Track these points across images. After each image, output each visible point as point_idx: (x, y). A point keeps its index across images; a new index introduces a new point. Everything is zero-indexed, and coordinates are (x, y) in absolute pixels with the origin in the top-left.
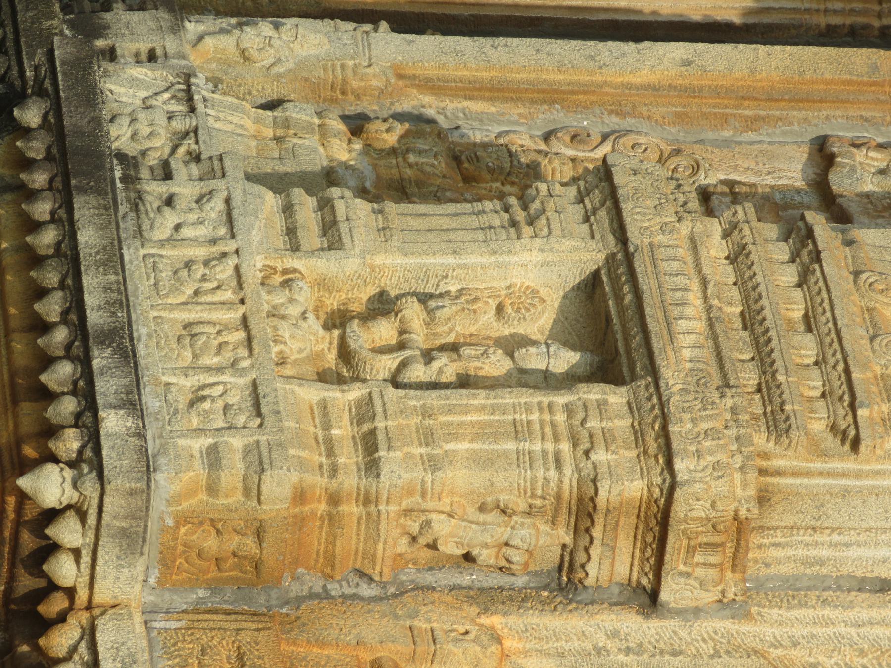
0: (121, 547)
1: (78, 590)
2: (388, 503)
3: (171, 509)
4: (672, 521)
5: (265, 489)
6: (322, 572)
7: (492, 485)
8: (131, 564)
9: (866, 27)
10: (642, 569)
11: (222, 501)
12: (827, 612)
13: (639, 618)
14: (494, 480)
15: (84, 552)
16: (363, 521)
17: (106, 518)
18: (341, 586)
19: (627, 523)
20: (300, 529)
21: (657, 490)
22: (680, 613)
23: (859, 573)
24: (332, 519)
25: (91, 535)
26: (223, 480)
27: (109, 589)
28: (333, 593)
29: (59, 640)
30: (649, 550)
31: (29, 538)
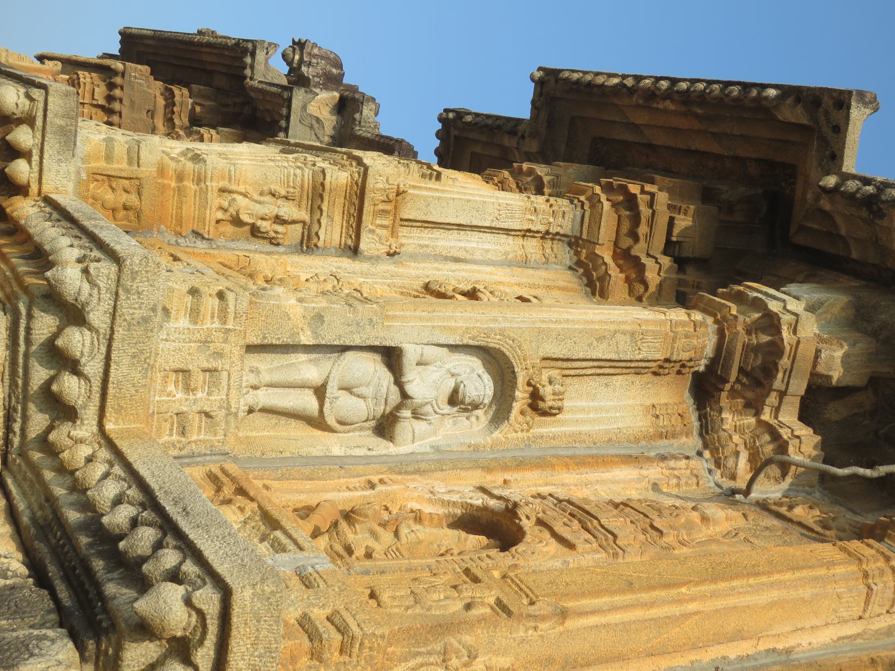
0: (60, 143)
3: (84, 166)
4: (367, 191)
5: (143, 155)
6: (175, 231)
10: (347, 233)
11: (116, 166)
12: (436, 265)
13: (350, 261)
14: (267, 174)
15: (34, 151)
16: (198, 194)
17: (50, 115)
19: (340, 201)
20: (162, 194)
21: (357, 175)
23: (444, 253)
24: (180, 190)
25: (39, 135)
26: (116, 148)
27: (52, 181)
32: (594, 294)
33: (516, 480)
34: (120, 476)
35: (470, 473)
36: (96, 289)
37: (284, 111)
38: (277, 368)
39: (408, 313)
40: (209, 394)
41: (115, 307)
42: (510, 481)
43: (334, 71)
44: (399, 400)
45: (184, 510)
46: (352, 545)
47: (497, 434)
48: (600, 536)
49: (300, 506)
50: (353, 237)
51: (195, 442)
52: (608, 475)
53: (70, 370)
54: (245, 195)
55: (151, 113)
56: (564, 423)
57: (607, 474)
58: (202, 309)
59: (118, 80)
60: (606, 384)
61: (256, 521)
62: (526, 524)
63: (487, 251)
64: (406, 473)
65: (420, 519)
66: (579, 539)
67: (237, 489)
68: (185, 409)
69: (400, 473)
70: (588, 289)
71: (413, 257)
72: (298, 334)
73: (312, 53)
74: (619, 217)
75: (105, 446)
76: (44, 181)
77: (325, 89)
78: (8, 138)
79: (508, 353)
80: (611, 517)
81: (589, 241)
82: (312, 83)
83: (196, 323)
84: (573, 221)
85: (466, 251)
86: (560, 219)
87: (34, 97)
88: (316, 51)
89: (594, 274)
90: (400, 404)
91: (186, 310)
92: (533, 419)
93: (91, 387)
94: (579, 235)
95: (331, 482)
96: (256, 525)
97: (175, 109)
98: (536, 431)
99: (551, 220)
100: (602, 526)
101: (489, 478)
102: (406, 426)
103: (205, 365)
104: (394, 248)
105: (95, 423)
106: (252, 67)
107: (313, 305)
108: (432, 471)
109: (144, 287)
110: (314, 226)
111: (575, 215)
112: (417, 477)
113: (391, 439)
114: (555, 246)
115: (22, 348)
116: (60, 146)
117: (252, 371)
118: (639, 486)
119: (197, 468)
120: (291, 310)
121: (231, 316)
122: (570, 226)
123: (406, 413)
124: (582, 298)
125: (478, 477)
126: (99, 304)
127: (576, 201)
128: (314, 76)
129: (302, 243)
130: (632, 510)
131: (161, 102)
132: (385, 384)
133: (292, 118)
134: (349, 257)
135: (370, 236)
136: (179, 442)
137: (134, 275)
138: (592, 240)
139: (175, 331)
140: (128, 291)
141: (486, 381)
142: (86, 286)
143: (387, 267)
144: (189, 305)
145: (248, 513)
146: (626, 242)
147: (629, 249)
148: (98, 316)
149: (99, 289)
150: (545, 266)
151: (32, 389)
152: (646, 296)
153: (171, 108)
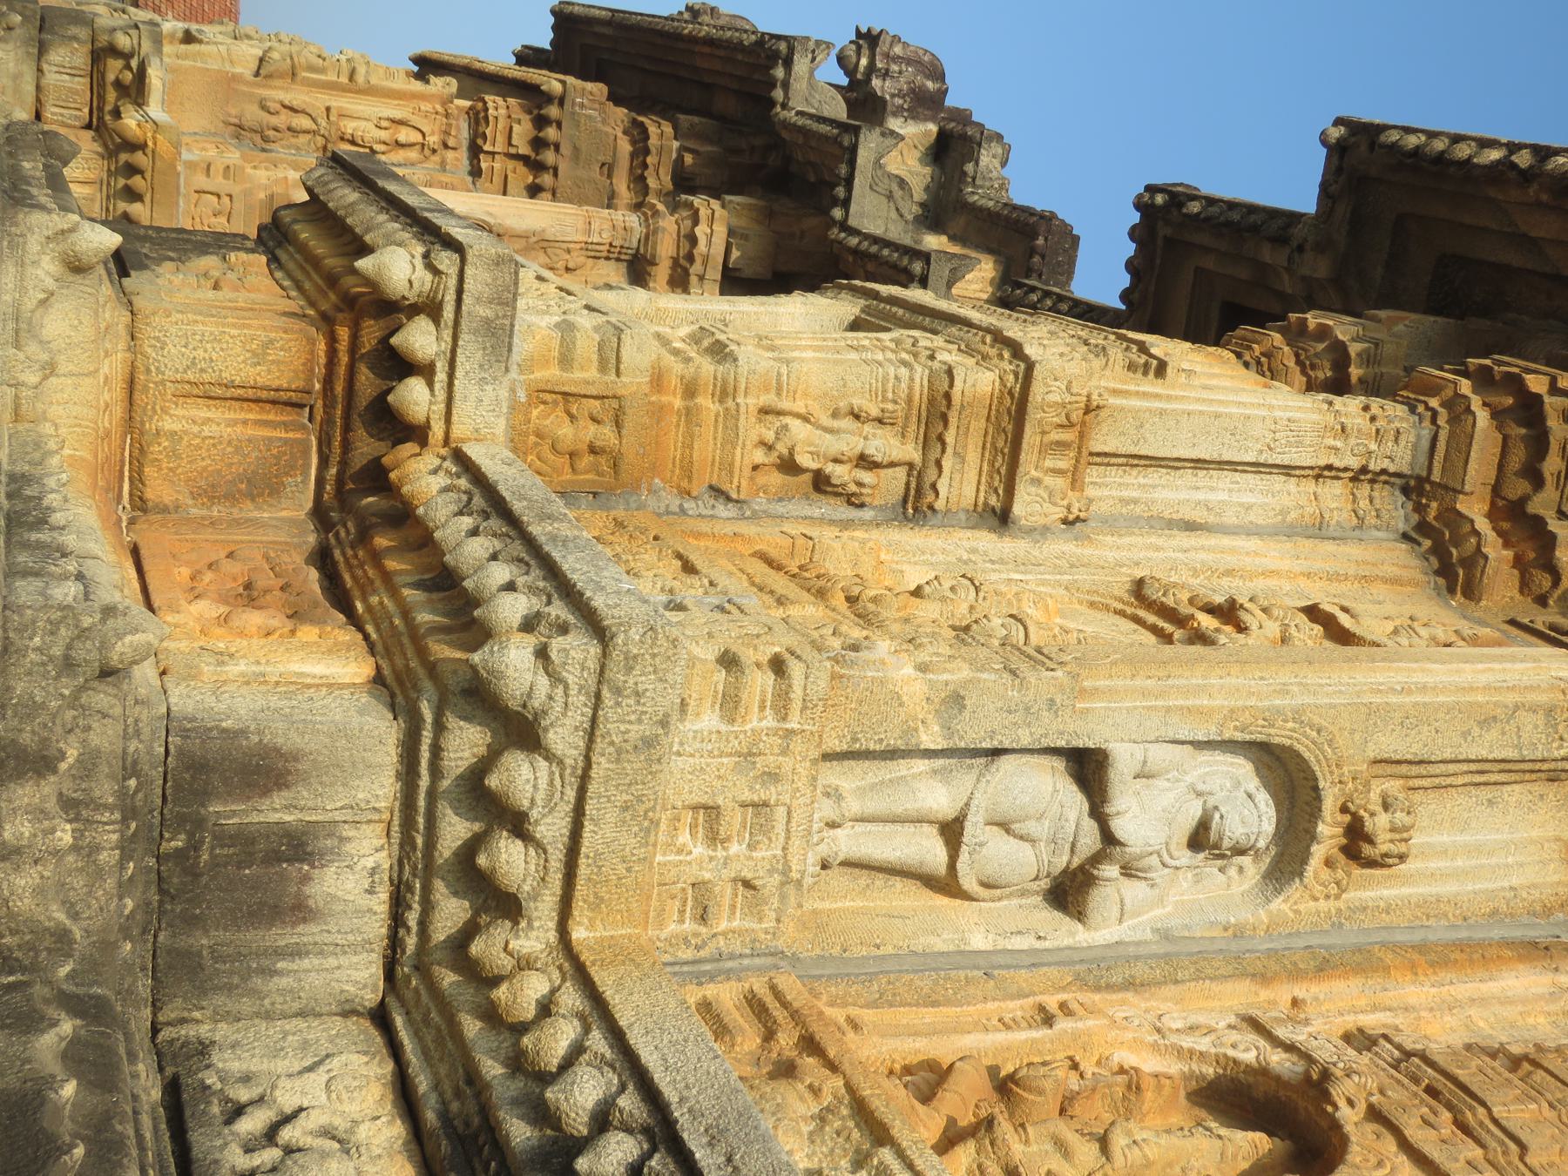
0: (484, 349)
1: (432, 423)
2: (745, 396)
3: (522, 378)
6: (679, 487)
7: (844, 386)
8: (495, 379)
10: (990, 485)
11: (578, 375)
12: (1153, 539)
13: (993, 536)
16: (721, 419)
17: (467, 299)
18: (698, 506)
20: (658, 423)
21: (1011, 377)
22: (1031, 531)
23: (1166, 515)
24: (690, 415)
25: (447, 335)
26: (579, 343)
27: (469, 417)
28: (690, 513)
29: (415, 466)
30: (1000, 459)
31: (367, 378)
32: (1451, 590)
33: (1316, 999)
34: (603, 1056)
35: (1229, 986)
36: (561, 687)
37: (843, 170)
38: (873, 787)
39: (1120, 682)
40: (752, 847)
41: (594, 720)
42: (1303, 1001)
43: (930, 85)
44: (1099, 846)
45: (729, 1160)
46: (1021, 1169)
47: (1278, 904)
48: (1493, 1144)
49: (913, 1060)
50: (1001, 492)
51: (724, 934)
52: (1492, 987)
53: (510, 827)
54: (805, 419)
55: (609, 169)
56: (1408, 879)
57: (1491, 984)
58: (744, 696)
59: (553, 111)
60: (1489, 801)
61: (843, 1119)
62: (1349, 1117)
63: (1249, 508)
64: (1110, 988)
65: (1138, 1088)
66: (1457, 1160)
67: (802, 1038)
68: (707, 876)
69: (1097, 989)
70: (1441, 581)
71: (1112, 524)
72: (916, 730)
73: (892, 53)
74: (1505, 438)
75: (573, 978)
76: (455, 418)
77: (913, 118)
78: (393, 341)
79: (1306, 755)
80: (1513, 1102)
81: (1446, 488)
82: (889, 108)
83: (732, 721)
84: (1415, 447)
85: (1209, 509)
86: (1390, 444)
87: (441, 267)
88: (898, 50)
89: (1454, 551)
90: (1098, 852)
91: (715, 697)
92: (1349, 875)
93: (546, 861)
94: (1424, 474)
95: (971, 1008)
96: (845, 1127)
97: (649, 160)
98: (1353, 896)
99: (1373, 446)
100: (1495, 1122)
101: (1265, 994)
102: (1111, 889)
103: (747, 796)
104: (1075, 512)
105: (552, 925)
106: (786, 85)
107: (946, 677)
108: (1159, 984)
109: (647, 683)
110: (928, 471)
111: (1419, 437)
112: (1129, 996)
113: (1080, 916)
114: (1376, 494)
115: (424, 782)
116: (484, 355)
117: (828, 795)
118: (1552, 1008)
119: (727, 985)
120: (905, 689)
121: (796, 705)
122: (1408, 458)
123: (1110, 871)
124: (1430, 599)
125: (1241, 995)
126: (564, 714)
127: (1421, 408)
128: (893, 96)
129: (905, 501)
130: (1549, 1078)
131: (625, 147)
132: (1072, 816)
133: (857, 181)
134: (992, 530)
135: (1033, 490)
136: (696, 935)
137: (630, 662)
138: (1451, 484)
139: (695, 738)
140: (618, 691)
141: (1262, 806)
142: (543, 682)
143: (1062, 546)
144: (720, 688)
145: (827, 1099)
146: (1517, 488)
147: (1524, 500)
148: (563, 737)
149: (566, 687)
150: (1357, 533)
151: (441, 855)
152: (1555, 596)
153: (641, 158)
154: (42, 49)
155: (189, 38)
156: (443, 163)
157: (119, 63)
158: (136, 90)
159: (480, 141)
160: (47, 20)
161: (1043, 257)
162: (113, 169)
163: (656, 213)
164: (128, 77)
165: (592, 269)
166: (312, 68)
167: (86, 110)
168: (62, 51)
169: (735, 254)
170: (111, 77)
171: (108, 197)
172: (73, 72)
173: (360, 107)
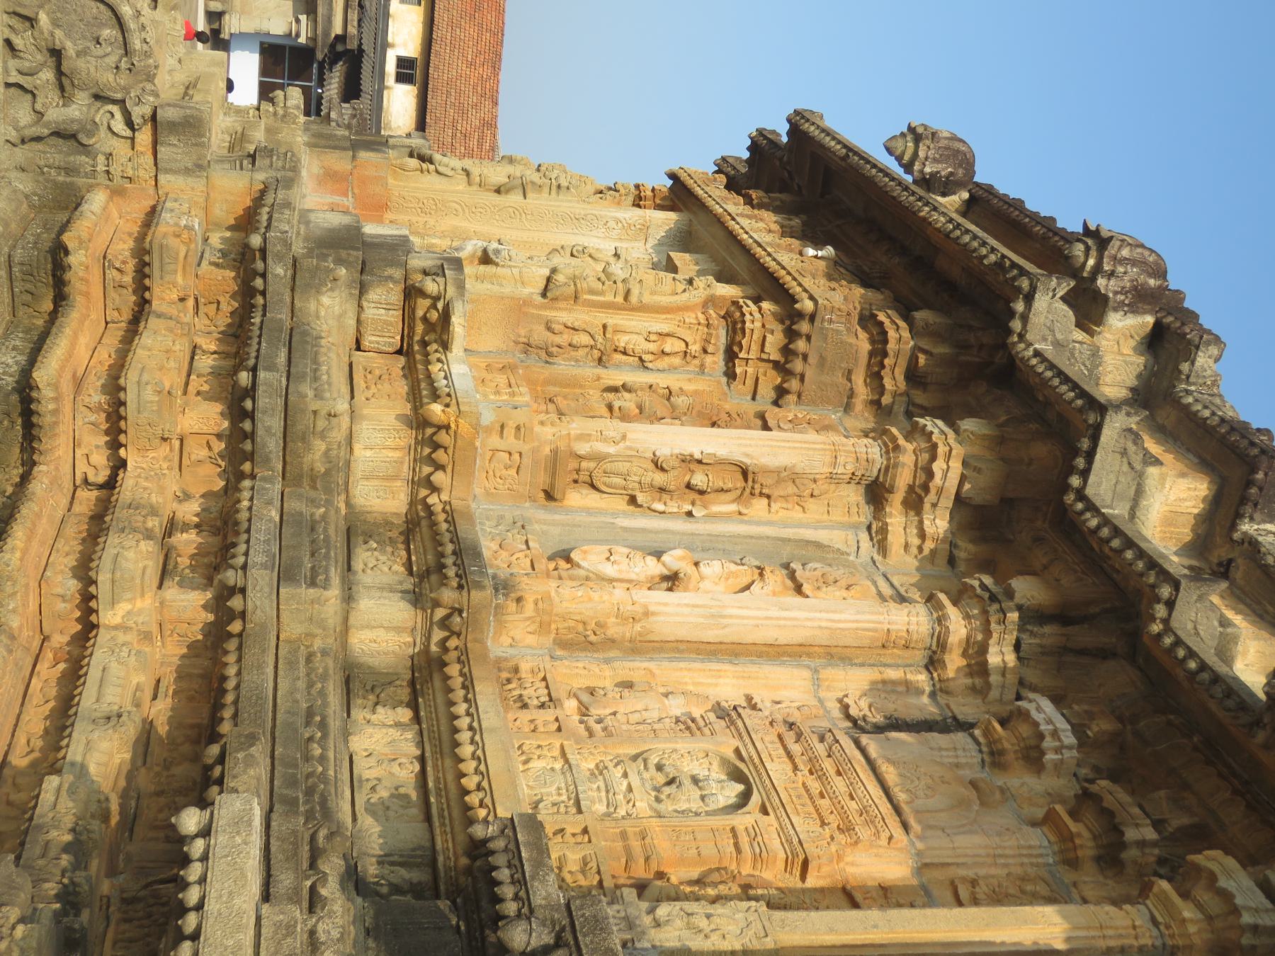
9: (1131, 947)
37: (1085, 444)
43: (1152, 282)
59: (804, 327)
73: (1119, 256)
77: (1133, 312)
82: (1111, 304)
88: (1125, 252)
97: (886, 361)
106: (1025, 318)
128: (1116, 293)
133: (1098, 457)
153: (879, 358)
154: (363, 289)
155: (486, 259)
156: (702, 366)
157: (428, 302)
158: (440, 329)
159: (736, 349)
160: (368, 264)
161: (1261, 489)
162: (420, 438)
163: (897, 448)
164: (434, 316)
165: (834, 492)
166: (592, 292)
167: (399, 338)
168: (379, 291)
169: (967, 486)
170: (420, 313)
171: (415, 460)
172: (388, 307)
173: (633, 323)
